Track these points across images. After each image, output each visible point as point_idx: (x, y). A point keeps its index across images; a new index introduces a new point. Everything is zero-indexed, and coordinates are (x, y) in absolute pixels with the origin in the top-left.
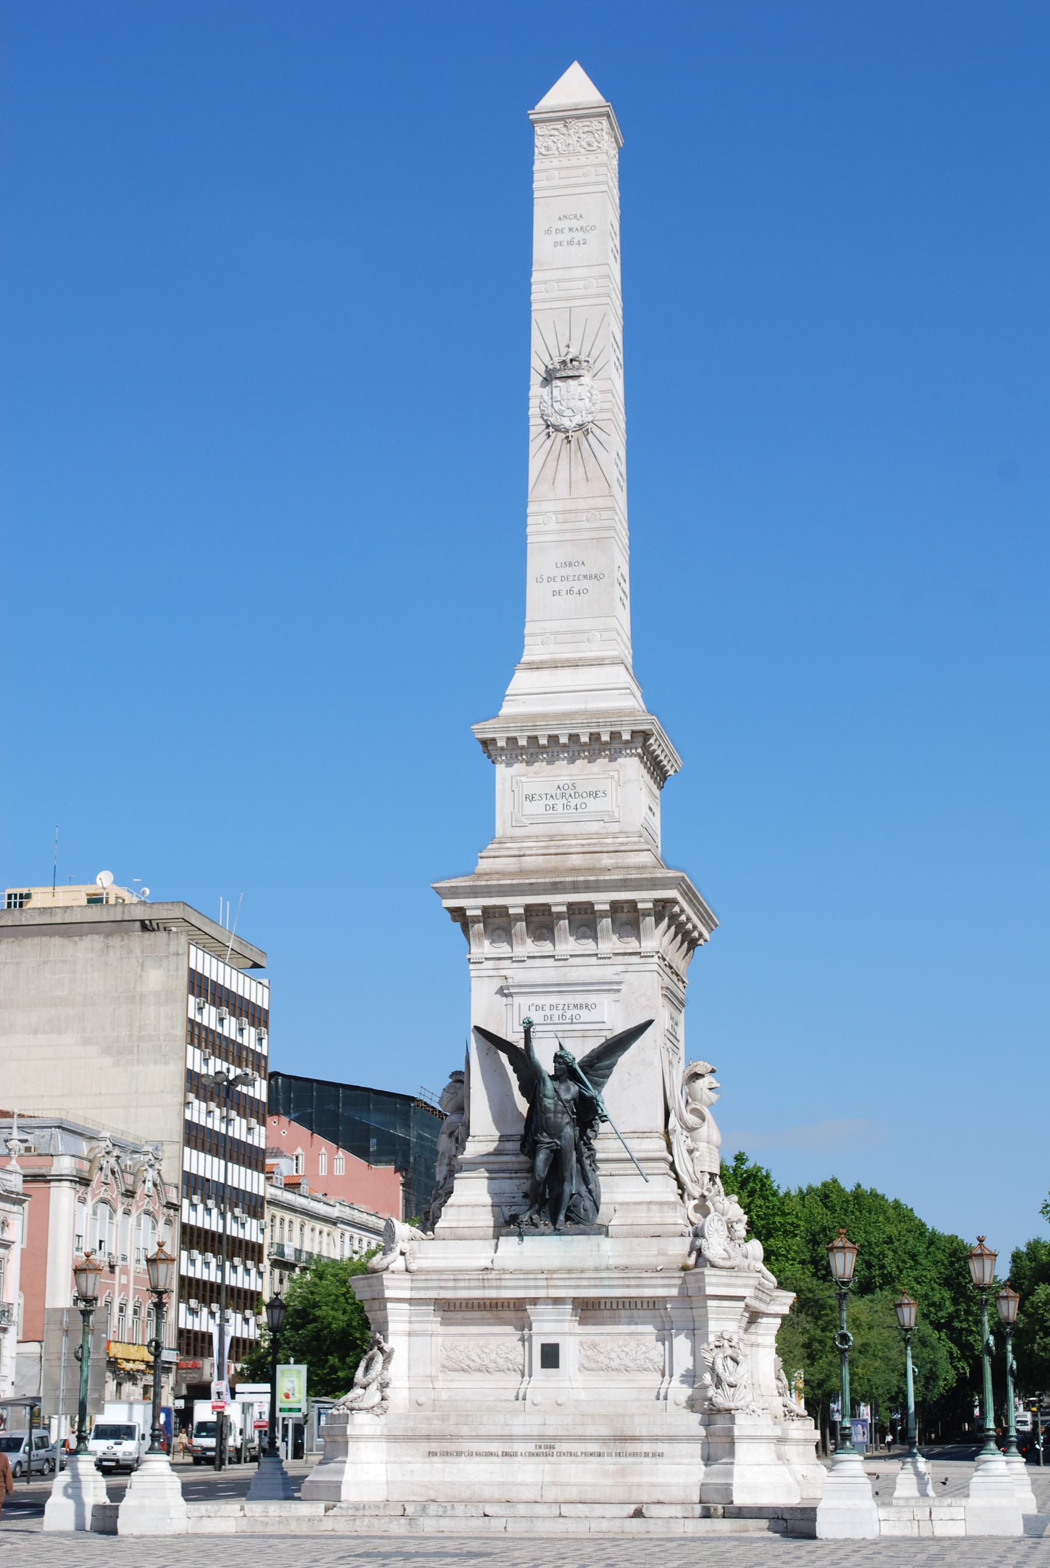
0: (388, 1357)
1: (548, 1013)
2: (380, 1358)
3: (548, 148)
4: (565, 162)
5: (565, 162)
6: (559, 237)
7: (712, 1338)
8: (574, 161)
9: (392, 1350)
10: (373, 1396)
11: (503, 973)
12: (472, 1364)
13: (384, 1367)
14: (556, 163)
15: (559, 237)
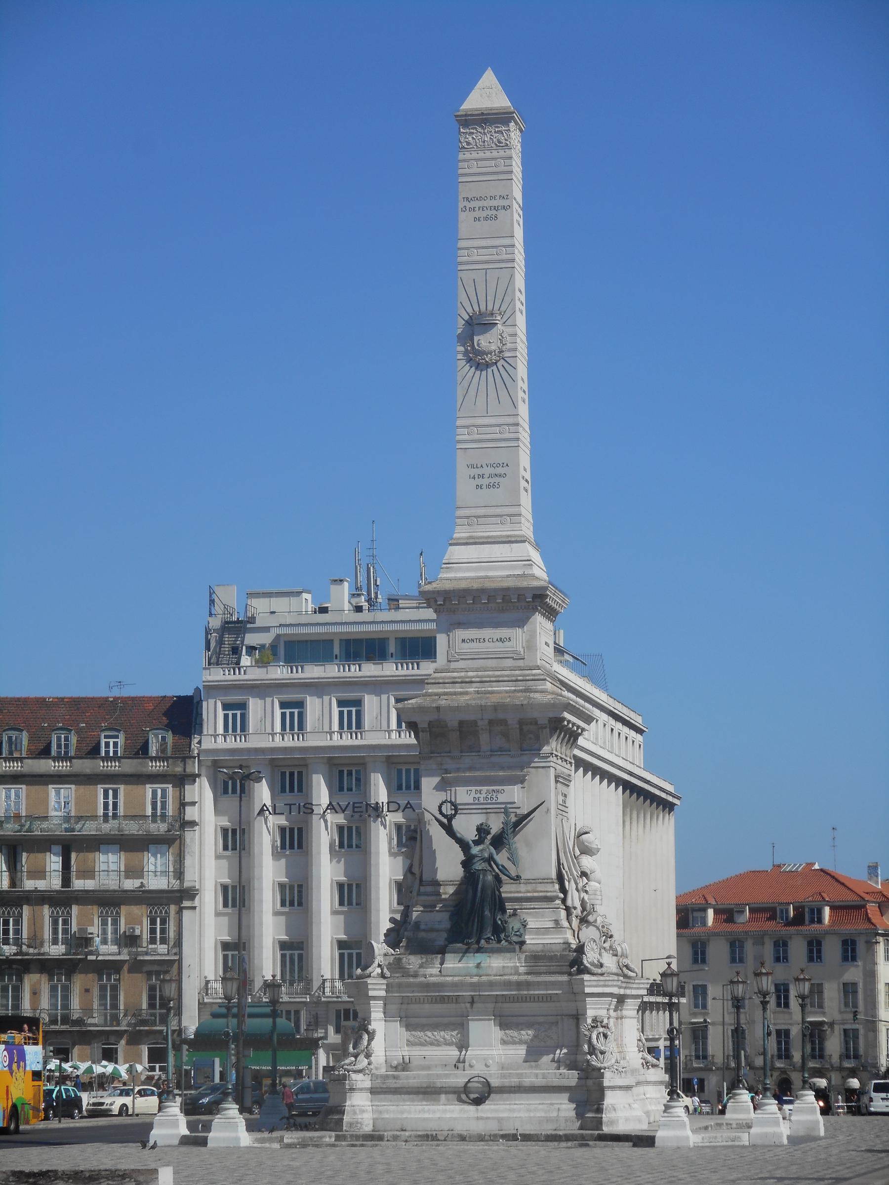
0: (371, 1035)
1: (477, 796)
2: (366, 1037)
3: (468, 143)
4: (481, 155)
5: (481, 155)
6: (477, 214)
7: (589, 1021)
8: (488, 154)
9: (374, 1031)
10: (363, 1062)
11: (445, 767)
12: (428, 1039)
13: (369, 1044)
14: (474, 155)
15: (477, 214)
